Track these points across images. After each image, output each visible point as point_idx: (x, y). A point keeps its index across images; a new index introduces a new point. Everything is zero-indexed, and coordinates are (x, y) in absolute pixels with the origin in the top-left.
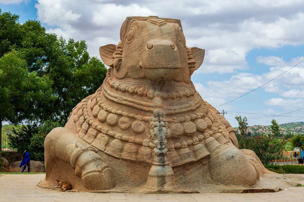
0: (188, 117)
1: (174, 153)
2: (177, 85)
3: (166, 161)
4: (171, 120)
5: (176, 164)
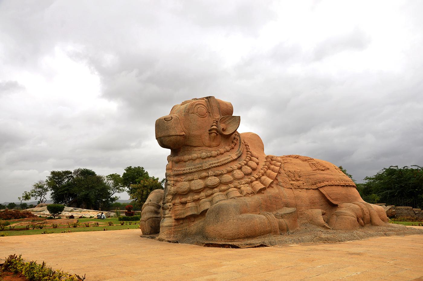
0: (196, 176)
1: (179, 207)
2: (194, 150)
3: (168, 214)
4: (179, 179)
5: (178, 217)
